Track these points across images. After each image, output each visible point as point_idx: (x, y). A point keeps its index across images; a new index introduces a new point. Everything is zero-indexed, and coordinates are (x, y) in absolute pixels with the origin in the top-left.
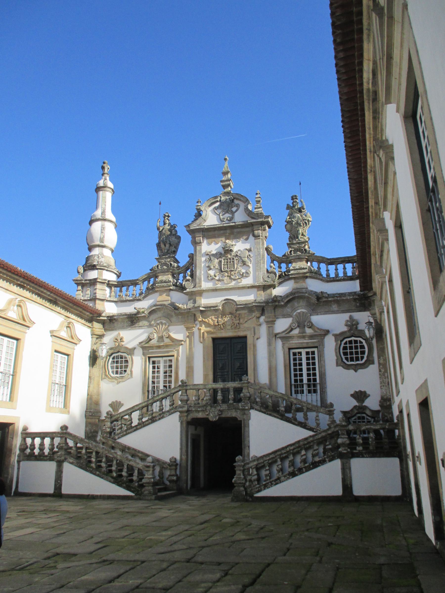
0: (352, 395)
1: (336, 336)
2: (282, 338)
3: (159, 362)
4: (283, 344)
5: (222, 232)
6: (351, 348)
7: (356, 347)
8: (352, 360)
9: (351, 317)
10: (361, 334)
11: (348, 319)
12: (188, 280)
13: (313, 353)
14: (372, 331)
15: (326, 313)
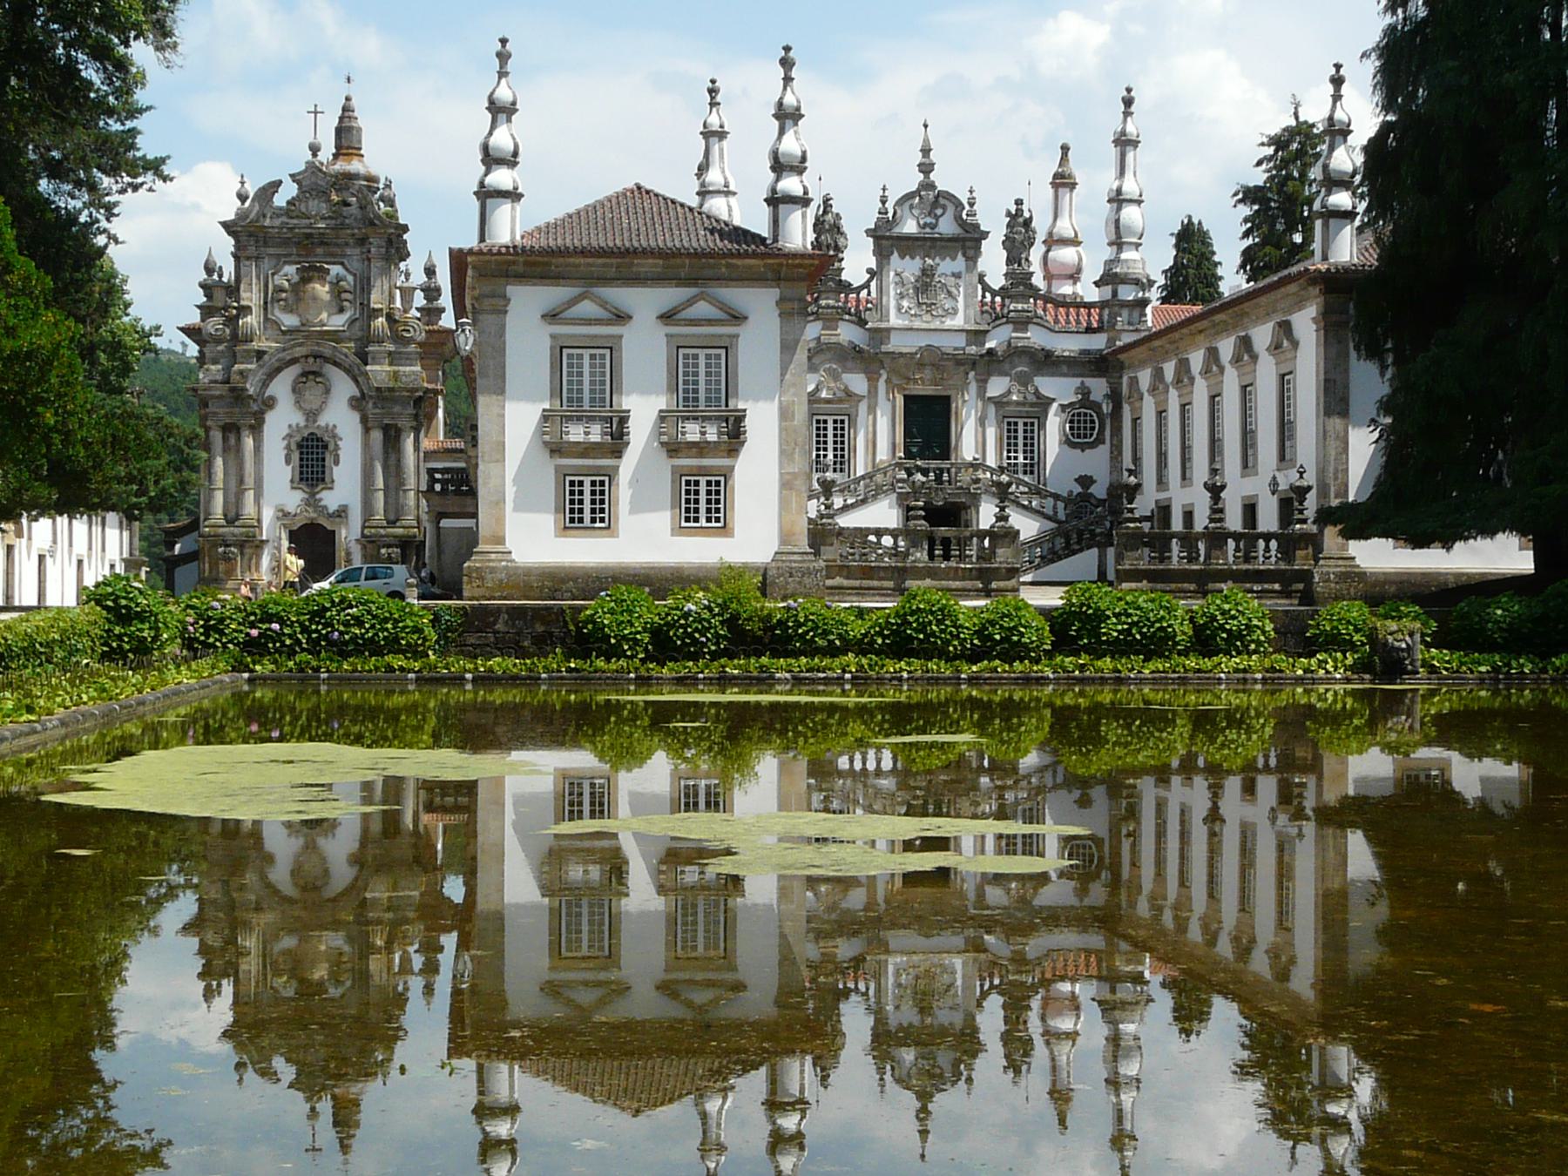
1: (1063, 407)
2: (995, 403)
4: (997, 411)
6: (1079, 422)
7: (1085, 422)
8: (1079, 437)
9: (1082, 383)
10: (1096, 407)
11: (1078, 385)
12: (870, 309)
13: (1032, 424)
15: (1053, 375)
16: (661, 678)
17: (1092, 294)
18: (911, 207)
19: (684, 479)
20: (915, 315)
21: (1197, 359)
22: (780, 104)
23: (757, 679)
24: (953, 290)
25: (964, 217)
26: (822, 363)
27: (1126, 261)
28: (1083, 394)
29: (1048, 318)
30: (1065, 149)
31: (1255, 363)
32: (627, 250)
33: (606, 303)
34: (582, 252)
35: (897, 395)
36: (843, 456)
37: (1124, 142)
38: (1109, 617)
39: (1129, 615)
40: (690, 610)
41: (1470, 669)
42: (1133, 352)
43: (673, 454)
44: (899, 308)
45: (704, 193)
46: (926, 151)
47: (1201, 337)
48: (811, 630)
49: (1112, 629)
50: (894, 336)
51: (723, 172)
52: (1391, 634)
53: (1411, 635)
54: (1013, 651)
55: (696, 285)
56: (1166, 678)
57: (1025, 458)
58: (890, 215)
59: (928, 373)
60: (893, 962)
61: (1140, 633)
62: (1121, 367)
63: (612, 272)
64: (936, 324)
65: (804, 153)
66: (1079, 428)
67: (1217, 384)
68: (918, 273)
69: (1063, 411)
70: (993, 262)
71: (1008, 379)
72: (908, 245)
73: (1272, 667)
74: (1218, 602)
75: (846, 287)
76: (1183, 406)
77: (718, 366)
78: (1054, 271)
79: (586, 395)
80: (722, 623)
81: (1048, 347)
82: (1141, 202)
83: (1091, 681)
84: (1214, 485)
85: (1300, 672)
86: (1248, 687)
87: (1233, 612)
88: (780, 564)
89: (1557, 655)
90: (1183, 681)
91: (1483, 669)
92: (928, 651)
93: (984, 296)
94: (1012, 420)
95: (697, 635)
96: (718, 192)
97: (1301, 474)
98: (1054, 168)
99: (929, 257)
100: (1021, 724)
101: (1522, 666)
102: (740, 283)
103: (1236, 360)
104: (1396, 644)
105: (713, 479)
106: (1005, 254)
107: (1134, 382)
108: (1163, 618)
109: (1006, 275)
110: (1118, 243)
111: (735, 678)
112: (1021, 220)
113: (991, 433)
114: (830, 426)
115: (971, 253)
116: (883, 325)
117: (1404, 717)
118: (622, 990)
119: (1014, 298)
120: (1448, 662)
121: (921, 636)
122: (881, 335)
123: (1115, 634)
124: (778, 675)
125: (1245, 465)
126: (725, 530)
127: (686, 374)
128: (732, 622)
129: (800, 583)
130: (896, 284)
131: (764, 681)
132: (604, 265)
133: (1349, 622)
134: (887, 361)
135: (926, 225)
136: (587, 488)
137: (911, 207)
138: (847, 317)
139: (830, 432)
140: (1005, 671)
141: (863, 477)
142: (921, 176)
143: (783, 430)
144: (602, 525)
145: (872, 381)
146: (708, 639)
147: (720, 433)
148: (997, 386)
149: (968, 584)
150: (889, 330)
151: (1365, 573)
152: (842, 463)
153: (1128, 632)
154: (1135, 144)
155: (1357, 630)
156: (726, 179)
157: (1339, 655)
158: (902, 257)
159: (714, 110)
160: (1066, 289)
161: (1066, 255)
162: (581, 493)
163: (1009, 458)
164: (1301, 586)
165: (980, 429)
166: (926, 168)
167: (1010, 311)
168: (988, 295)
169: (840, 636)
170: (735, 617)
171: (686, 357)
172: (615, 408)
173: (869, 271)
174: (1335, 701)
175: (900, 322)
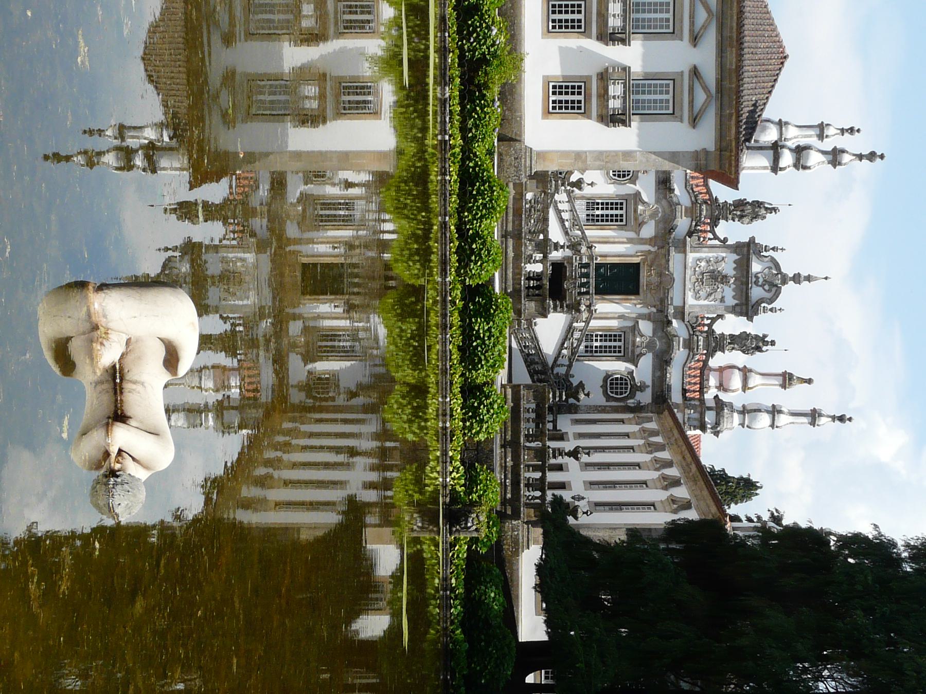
0: (581, 382)
1: (631, 373)
3: (621, 209)
5: (745, 273)
6: (621, 384)
7: (621, 388)
8: (611, 384)
9: (648, 386)
10: (632, 395)
11: (647, 384)
12: (699, 240)
13: (620, 352)
14: (633, 405)
16: (445, 6)
17: (709, 395)
18: (770, 268)
19: (583, 84)
20: (695, 271)
21: (665, 455)
22: (843, 151)
23: (445, 74)
24: (713, 297)
25: (763, 305)
26: (663, 207)
27: (732, 417)
28: (640, 386)
29: (693, 363)
30: (809, 381)
31: (662, 489)
32: (742, 43)
33: (705, 29)
34: (741, 12)
35: (640, 258)
36: (598, 221)
37: (814, 416)
38: (488, 324)
39: (489, 338)
40: (492, 31)
41: (453, 572)
42: (669, 419)
43: (600, 77)
44: (700, 260)
45: (781, 124)
46: (809, 278)
47: (680, 458)
48: (478, 116)
49: (480, 326)
50: (681, 256)
51: (795, 138)
52: (477, 516)
53: (477, 530)
54: (465, 256)
55: (717, 92)
56: (446, 360)
57: (596, 347)
58: (764, 254)
59: (655, 279)
60: (250, 257)
61: (477, 346)
62: (659, 413)
63: (727, 33)
64: (689, 285)
65: (809, 168)
66: (617, 384)
67: (648, 467)
68: (724, 272)
69: (629, 373)
70: (731, 325)
71: (651, 335)
72: (743, 266)
73: (454, 436)
74: (499, 401)
75: (714, 223)
76: (632, 448)
77: (661, 108)
78: (725, 373)
79: (641, 16)
80: (484, 53)
81: (673, 363)
82: (773, 428)
83: (444, 307)
84: (578, 452)
85: (451, 454)
86: (441, 417)
87: (492, 411)
88: (523, 151)
89: (463, 632)
90: (444, 372)
91: (453, 581)
92: (464, 196)
93: (708, 318)
94: (623, 338)
95: (475, 35)
96: (781, 134)
97: (586, 513)
98: (796, 374)
99: (735, 281)
100: (415, 262)
101: (456, 608)
102: (719, 122)
103: (664, 478)
104: (470, 520)
105: (583, 105)
106: (737, 333)
107: (650, 420)
108: (488, 361)
109: (723, 334)
110: (744, 411)
111: (446, 59)
112: (761, 344)
113: (614, 323)
114: (619, 212)
115: (738, 309)
116: (688, 248)
117: (420, 525)
118: (228, 40)
119: (707, 339)
120: (458, 556)
121: (474, 192)
122: (682, 247)
123: (476, 328)
124: (447, 88)
125: (592, 484)
126: (547, 113)
127: (655, 86)
128: (484, 61)
129: (511, 164)
130: (717, 258)
131: (443, 79)
132: (732, 28)
133: (485, 491)
134: (663, 251)
135: (757, 278)
136: (576, 16)
137: (770, 268)
138: (694, 224)
139: (614, 212)
140: (450, 249)
141: (583, 233)
142: (791, 275)
143: (616, 153)
144: (550, 28)
145: (650, 241)
146: (472, 43)
147: (614, 109)
148: (646, 327)
149: (510, 282)
150: (685, 252)
151: (518, 556)
152: (593, 220)
153: (478, 337)
154: (813, 423)
155: (480, 497)
156: (790, 139)
157: (463, 482)
158: (735, 262)
159: (839, 131)
160: (713, 381)
161: (736, 381)
162: (573, 12)
163: (596, 336)
164: (509, 512)
165: (616, 316)
166: (797, 278)
167: (697, 336)
168: (709, 321)
169: (474, 137)
170: (488, 63)
171: (668, 85)
172: (632, 36)
173: (725, 240)
174: (431, 479)
175: (690, 260)
